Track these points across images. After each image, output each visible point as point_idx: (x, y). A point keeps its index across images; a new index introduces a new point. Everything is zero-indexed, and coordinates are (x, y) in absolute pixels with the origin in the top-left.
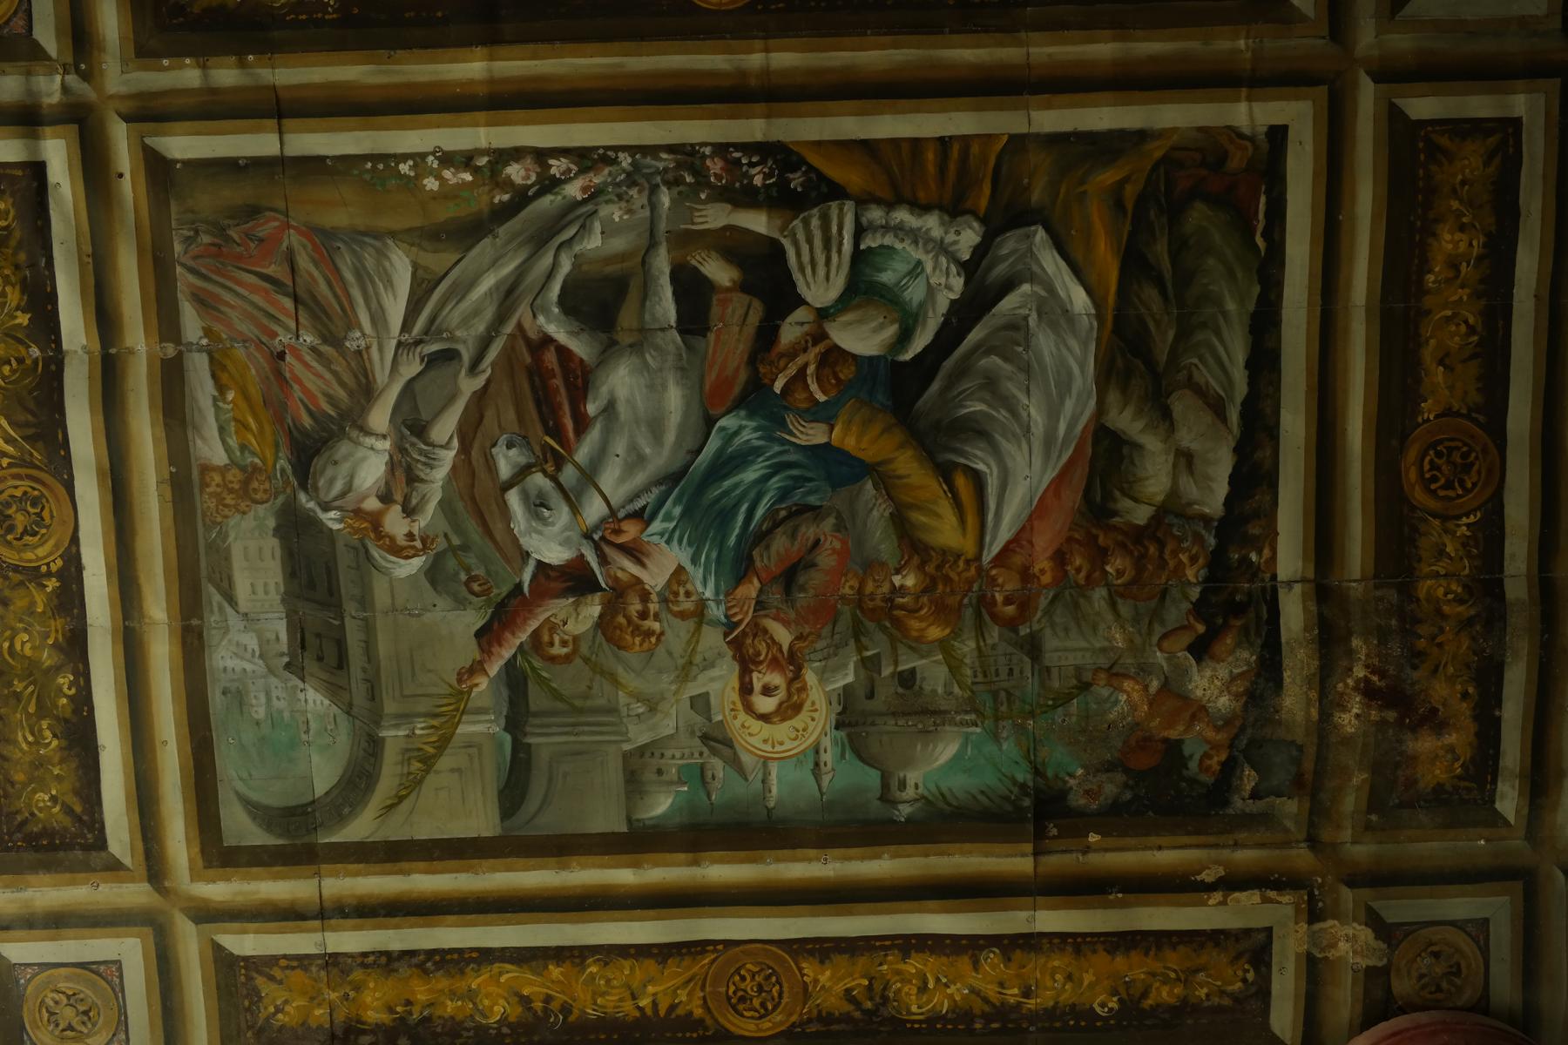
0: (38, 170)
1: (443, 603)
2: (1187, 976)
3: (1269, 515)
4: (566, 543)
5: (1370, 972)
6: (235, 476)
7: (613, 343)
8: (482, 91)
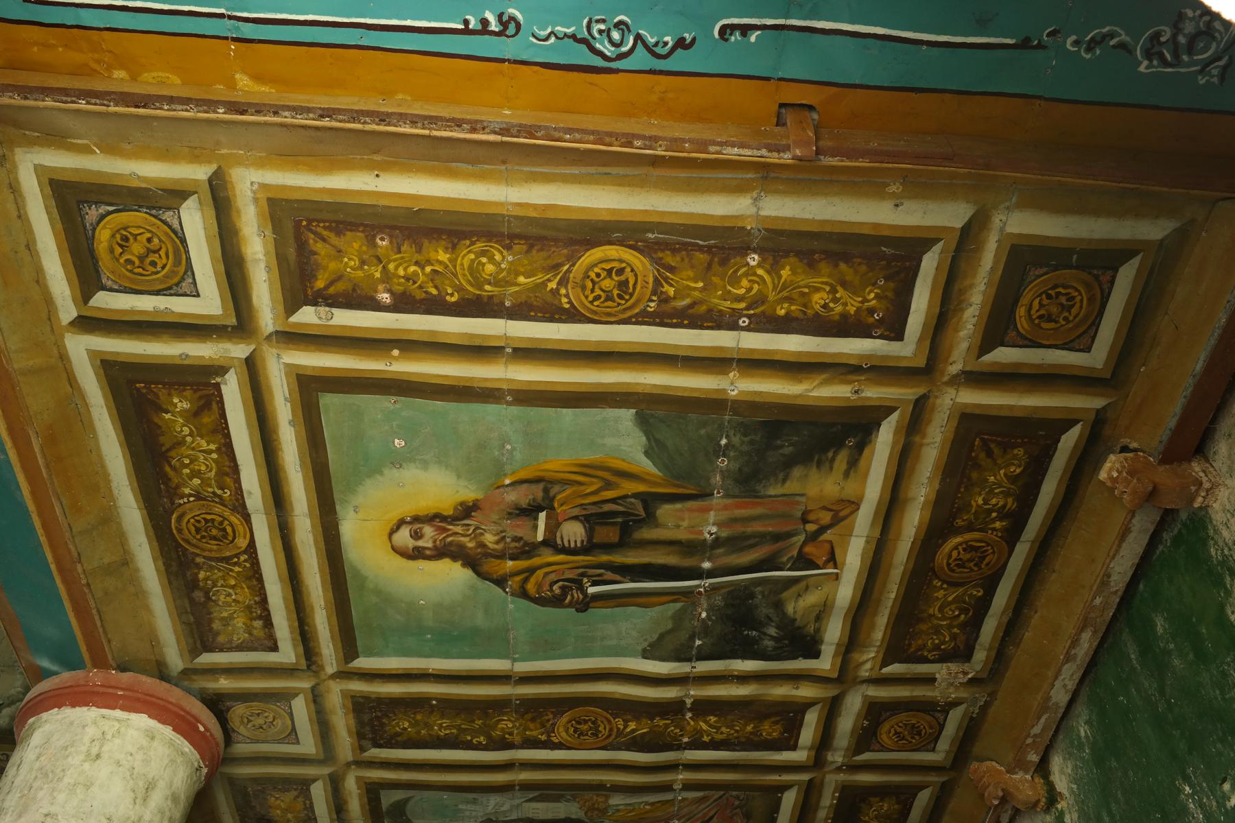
0: (794, 748)
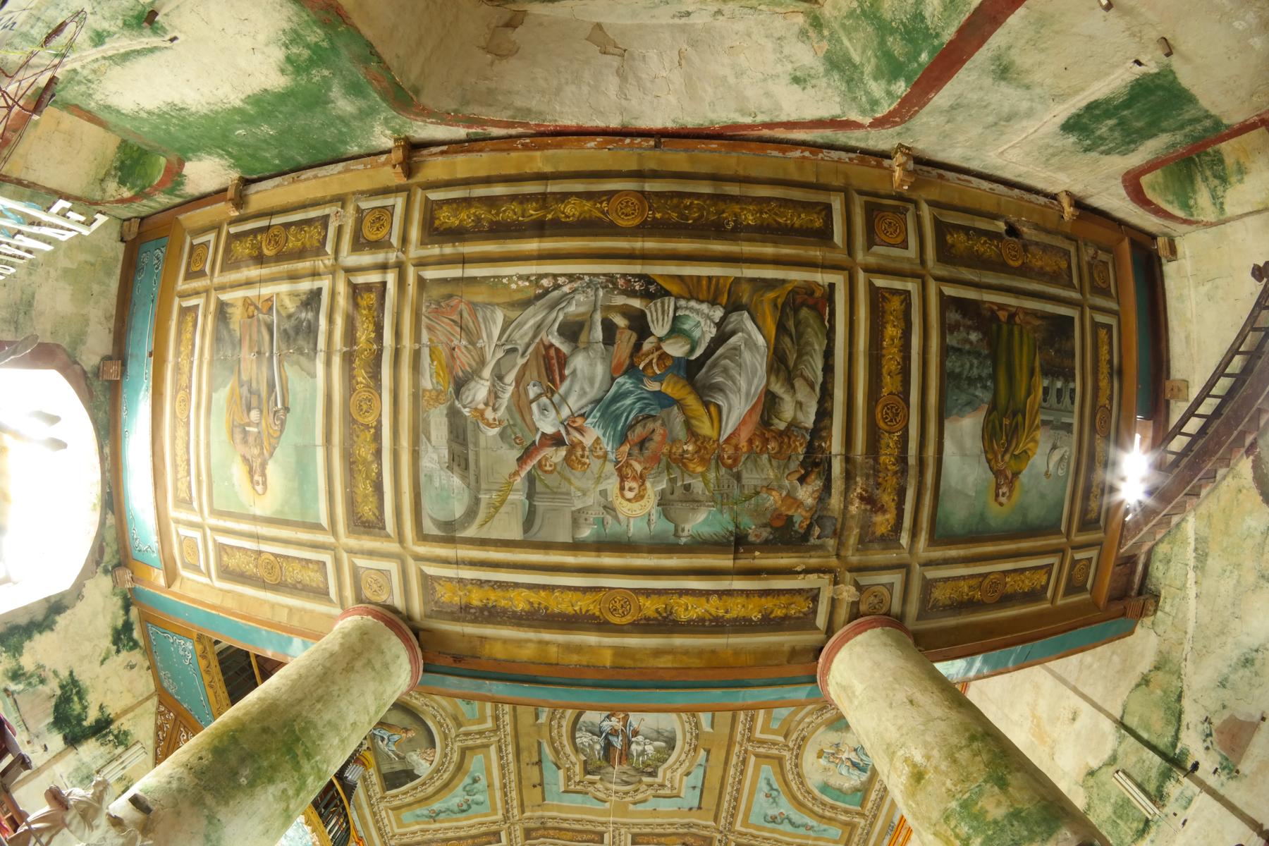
0: (384, 284)
1: (505, 446)
2: (787, 607)
3: (830, 428)
4: (553, 425)
5: (853, 603)
6: (434, 393)
7: (577, 347)
8: (535, 253)
